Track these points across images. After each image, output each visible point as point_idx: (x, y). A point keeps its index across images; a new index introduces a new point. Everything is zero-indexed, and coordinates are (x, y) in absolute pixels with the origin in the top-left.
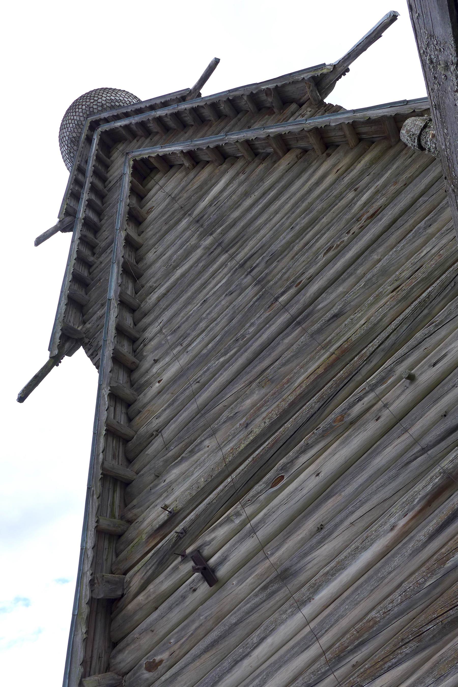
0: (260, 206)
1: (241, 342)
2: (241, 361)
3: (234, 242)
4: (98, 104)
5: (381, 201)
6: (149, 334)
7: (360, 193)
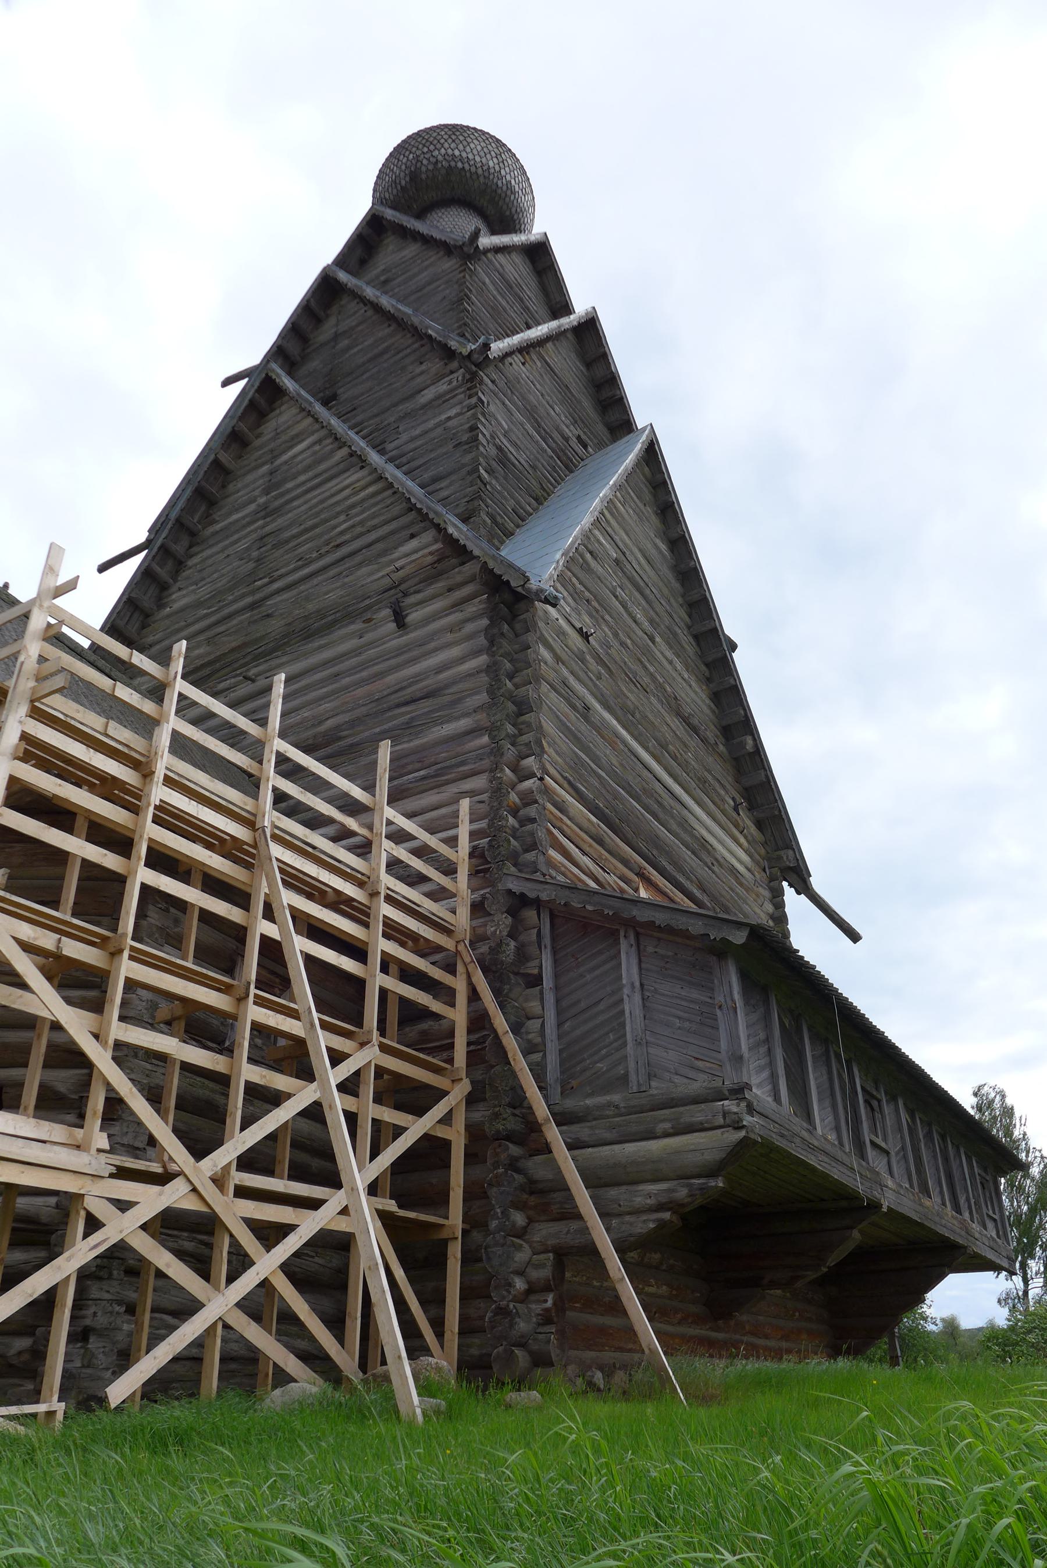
0: (304, 488)
1: (221, 604)
2: (213, 619)
3: (276, 510)
4: (431, 159)
5: (347, 537)
6: (190, 563)
7: (349, 517)
